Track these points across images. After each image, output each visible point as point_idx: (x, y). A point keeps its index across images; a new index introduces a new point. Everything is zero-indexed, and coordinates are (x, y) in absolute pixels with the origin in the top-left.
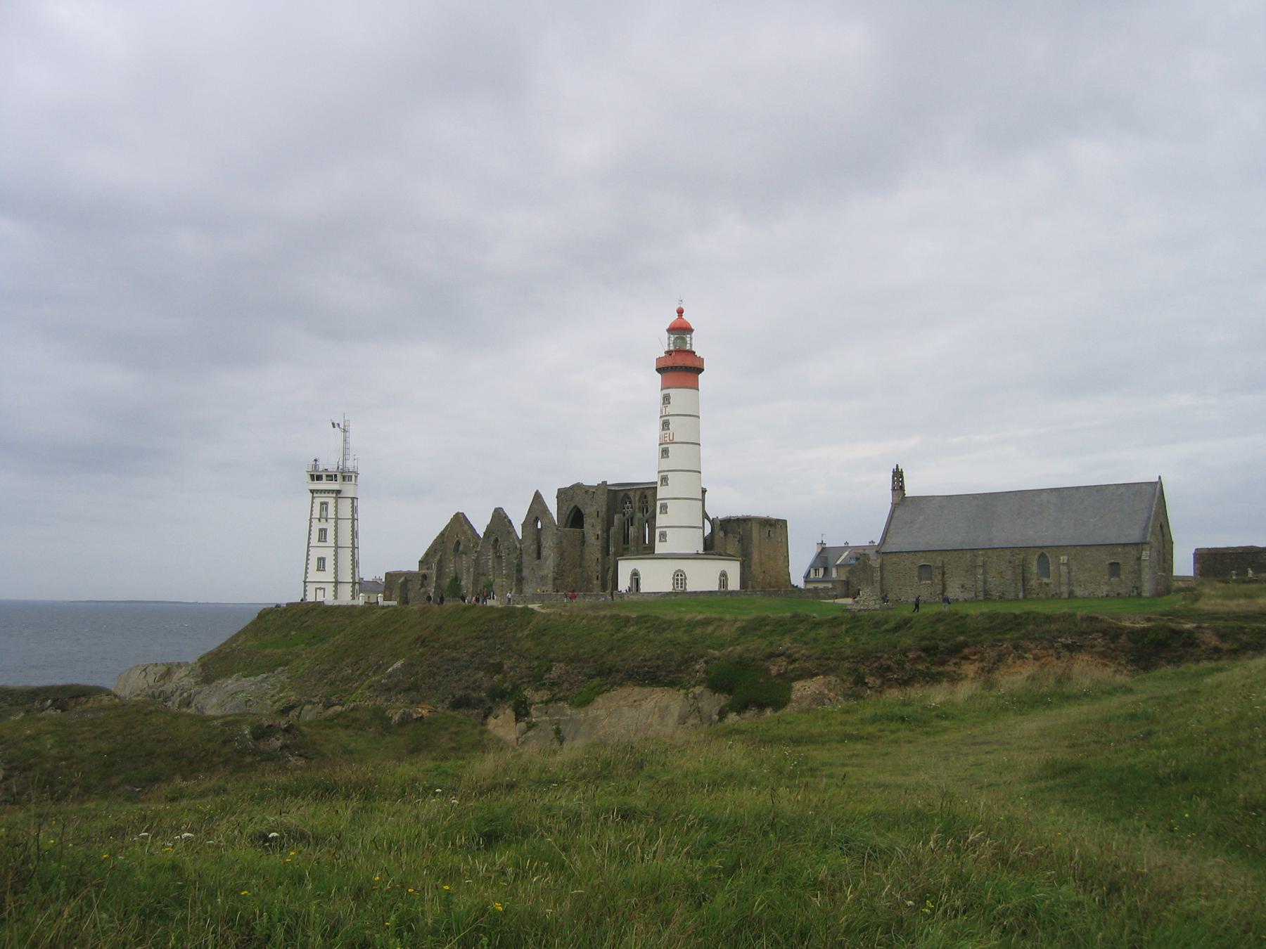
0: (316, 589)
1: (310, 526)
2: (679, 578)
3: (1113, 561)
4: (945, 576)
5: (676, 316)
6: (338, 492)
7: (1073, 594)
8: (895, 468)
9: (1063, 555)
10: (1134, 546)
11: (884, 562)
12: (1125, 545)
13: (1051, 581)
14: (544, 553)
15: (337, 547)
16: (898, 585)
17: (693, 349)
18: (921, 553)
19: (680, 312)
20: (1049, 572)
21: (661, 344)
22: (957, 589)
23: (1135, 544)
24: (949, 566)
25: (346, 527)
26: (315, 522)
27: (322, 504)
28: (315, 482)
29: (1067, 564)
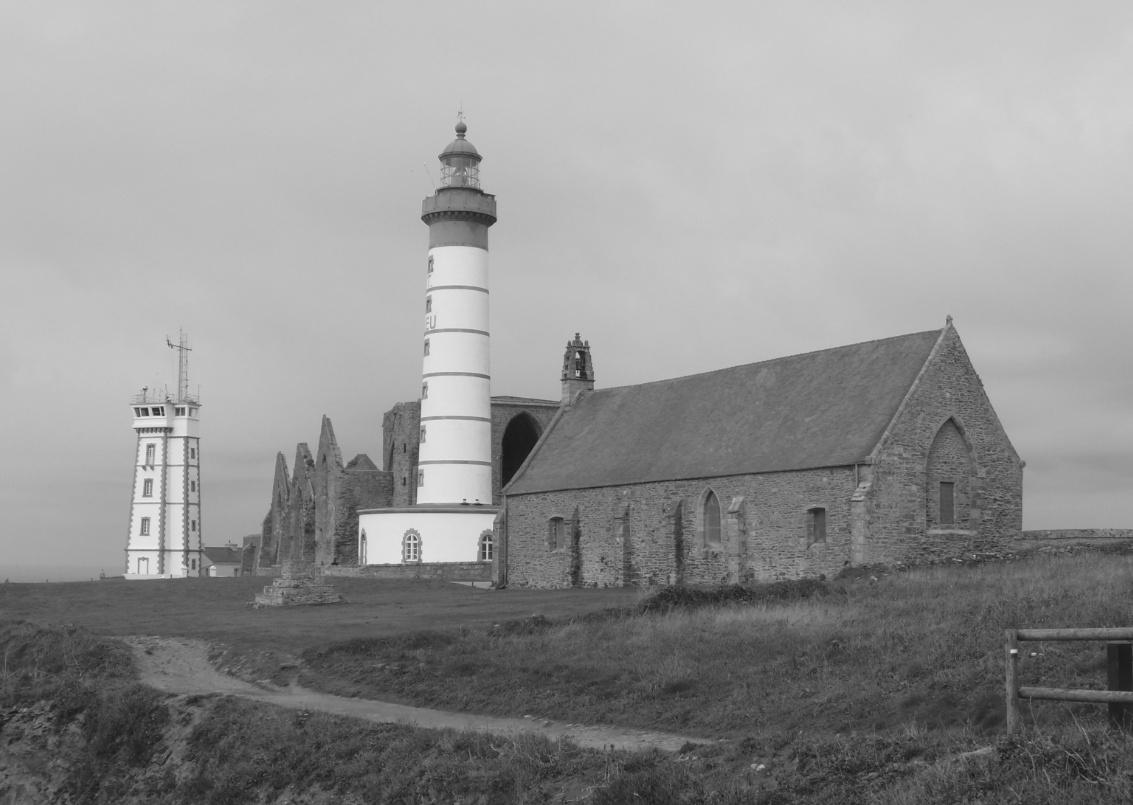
0: (139, 559)
1: (135, 476)
2: (412, 542)
3: (814, 506)
4: (581, 539)
5: (454, 136)
6: (168, 430)
7: (752, 575)
8: (572, 339)
9: (738, 493)
10: (848, 472)
11: (510, 514)
12: (832, 468)
13: (722, 549)
14: (331, 506)
15: (165, 503)
16: (525, 556)
17: (482, 188)
18: (551, 495)
19: (461, 131)
20: (720, 530)
21: (438, 176)
22: (596, 566)
23: (850, 467)
24: (587, 520)
25: (177, 477)
26: (140, 469)
27: (150, 446)
28: (142, 417)
29: (740, 514)
